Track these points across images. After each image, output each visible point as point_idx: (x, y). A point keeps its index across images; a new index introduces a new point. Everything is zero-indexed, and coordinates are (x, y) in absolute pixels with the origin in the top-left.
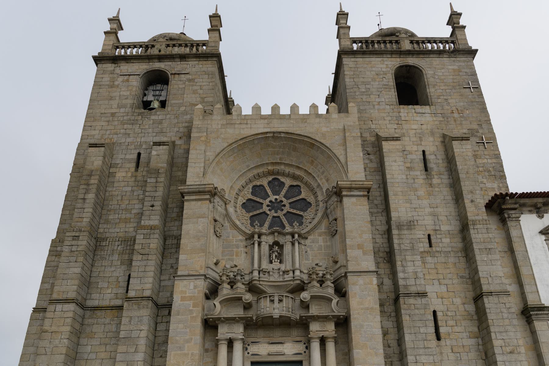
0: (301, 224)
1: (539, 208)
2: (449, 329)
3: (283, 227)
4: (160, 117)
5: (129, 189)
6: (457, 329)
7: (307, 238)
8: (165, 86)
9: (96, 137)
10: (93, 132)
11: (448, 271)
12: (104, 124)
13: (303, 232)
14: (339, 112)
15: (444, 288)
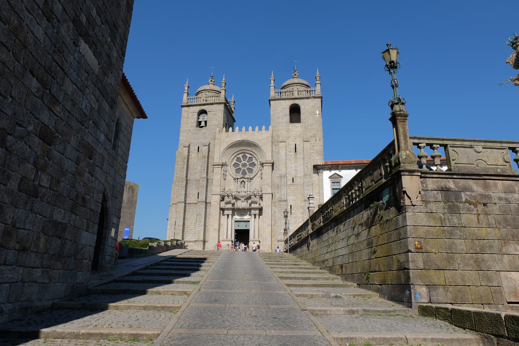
0: (252, 172)
1: (330, 169)
2: (294, 211)
3: (246, 174)
4: (205, 131)
5: (196, 161)
6: (297, 211)
7: (253, 179)
8: (206, 115)
9: (184, 140)
10: (183, 138)
11: (297, 191)
12: (186, 134)
13: (251, 177)
14: (266, 130)
15: (295, 197)
